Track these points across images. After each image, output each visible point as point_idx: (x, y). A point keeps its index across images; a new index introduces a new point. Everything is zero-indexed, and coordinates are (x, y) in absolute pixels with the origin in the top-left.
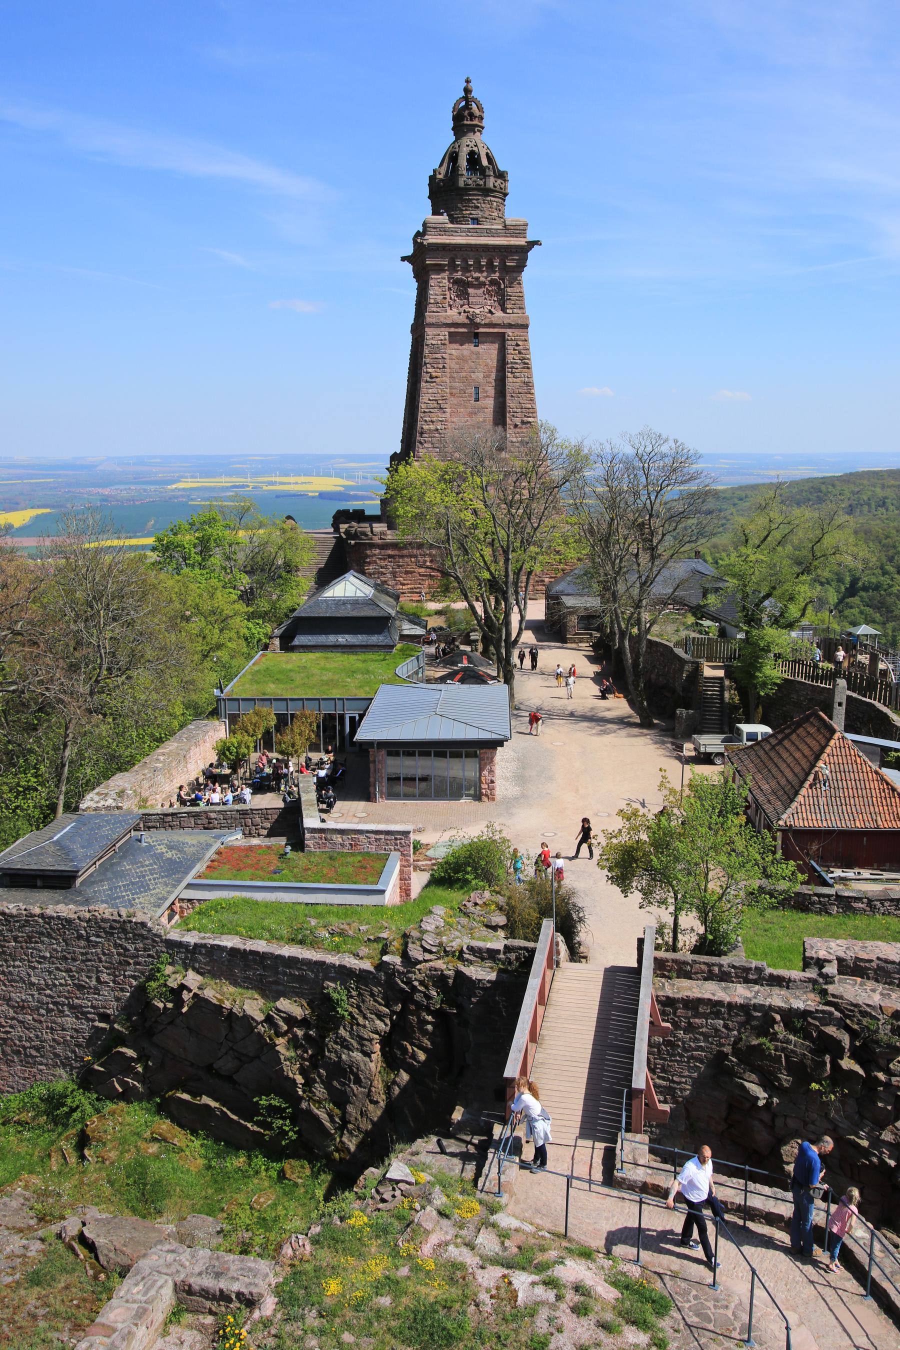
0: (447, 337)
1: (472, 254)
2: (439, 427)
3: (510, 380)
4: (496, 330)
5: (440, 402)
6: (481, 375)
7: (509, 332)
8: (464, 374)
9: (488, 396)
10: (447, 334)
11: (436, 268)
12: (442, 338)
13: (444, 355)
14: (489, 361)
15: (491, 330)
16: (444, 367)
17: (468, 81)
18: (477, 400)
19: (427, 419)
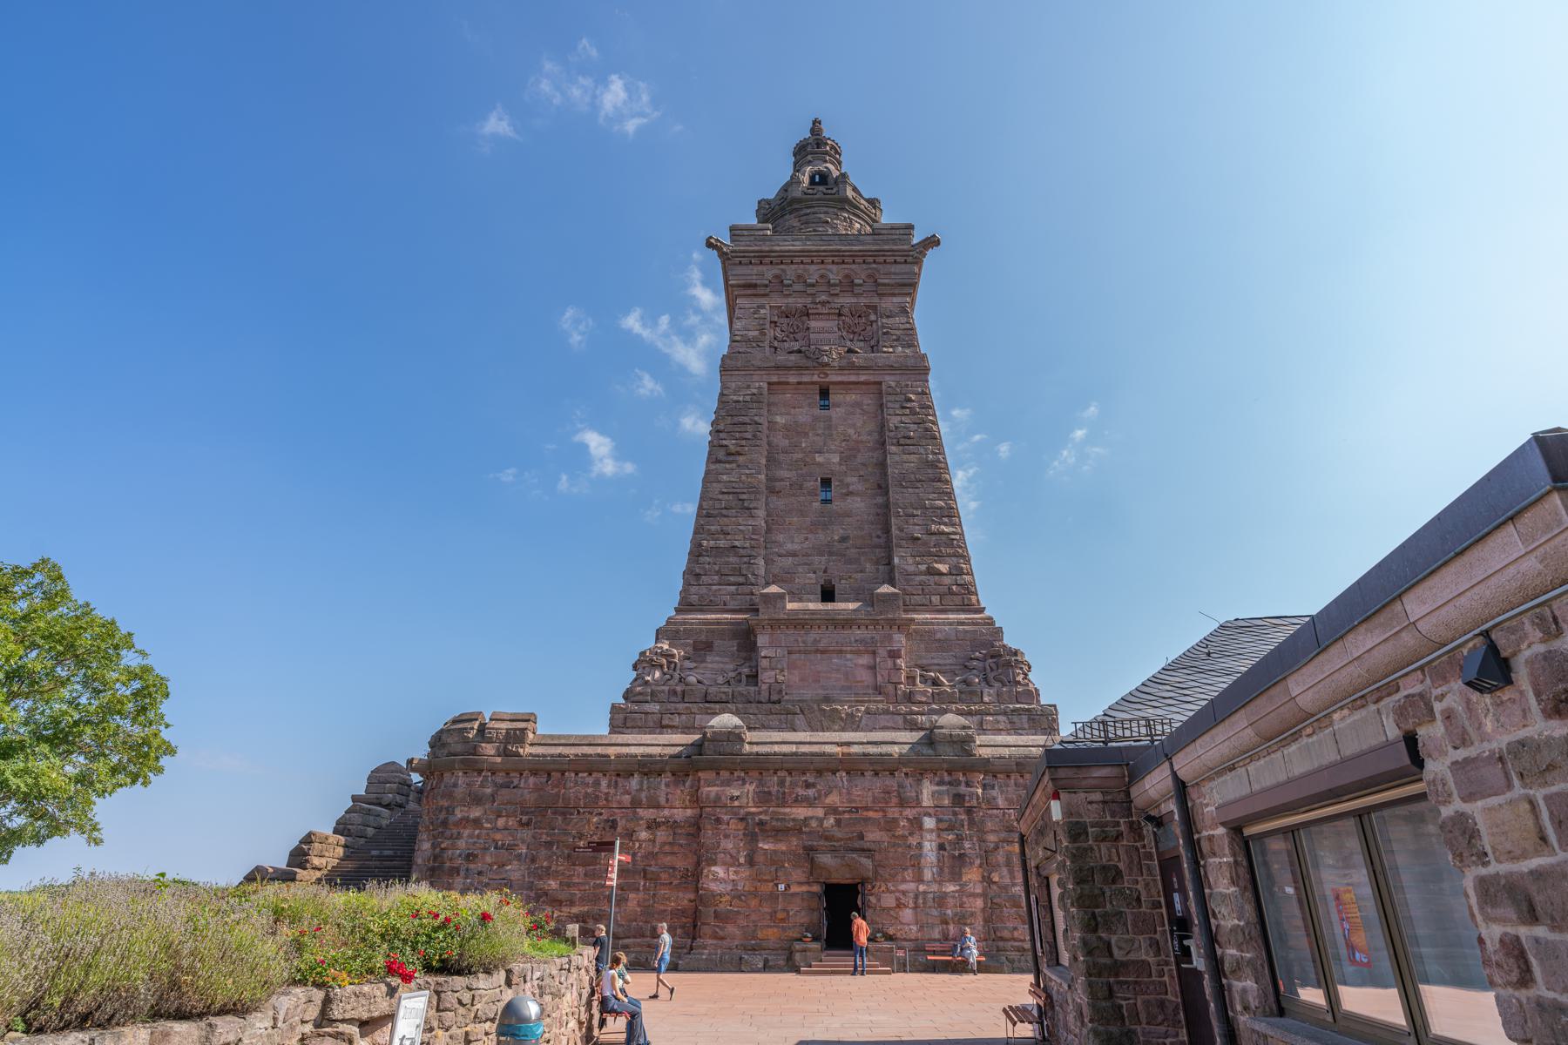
0: (765, 391)
1: (813, 268)
2: (737, 543)
3: (897, 458)
4: (862, 378)
5: (744, 497)
6: (836, 459)
7: (890, 380)
8: (800, 456)
9: (850, 494)
10: (765, 385)
11: (749, 292)
12: (755, 391)
13: (756, 418)
14: (851, 431)
15: (853, 378)
16: (754, 436)
17: (816, 122)
18: (826, 501)
19: (713, 528)
